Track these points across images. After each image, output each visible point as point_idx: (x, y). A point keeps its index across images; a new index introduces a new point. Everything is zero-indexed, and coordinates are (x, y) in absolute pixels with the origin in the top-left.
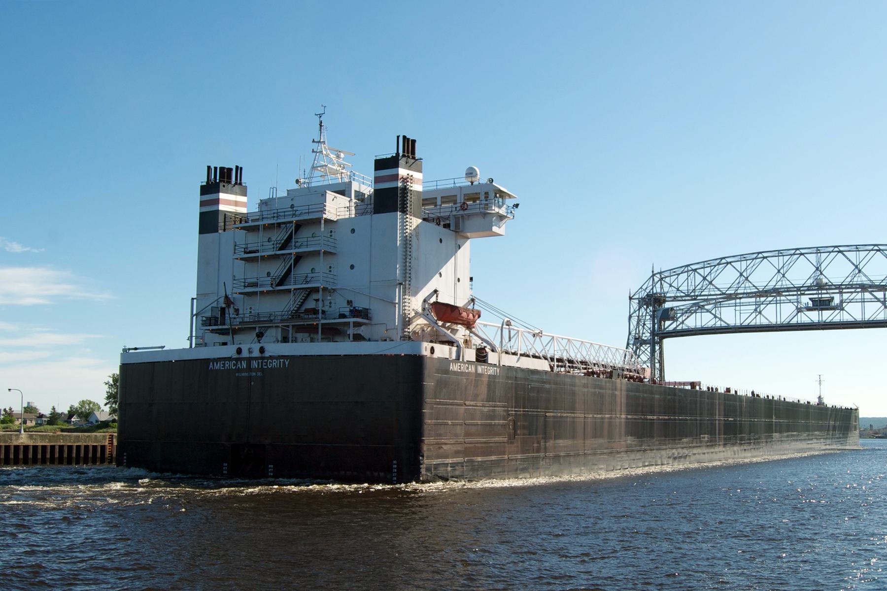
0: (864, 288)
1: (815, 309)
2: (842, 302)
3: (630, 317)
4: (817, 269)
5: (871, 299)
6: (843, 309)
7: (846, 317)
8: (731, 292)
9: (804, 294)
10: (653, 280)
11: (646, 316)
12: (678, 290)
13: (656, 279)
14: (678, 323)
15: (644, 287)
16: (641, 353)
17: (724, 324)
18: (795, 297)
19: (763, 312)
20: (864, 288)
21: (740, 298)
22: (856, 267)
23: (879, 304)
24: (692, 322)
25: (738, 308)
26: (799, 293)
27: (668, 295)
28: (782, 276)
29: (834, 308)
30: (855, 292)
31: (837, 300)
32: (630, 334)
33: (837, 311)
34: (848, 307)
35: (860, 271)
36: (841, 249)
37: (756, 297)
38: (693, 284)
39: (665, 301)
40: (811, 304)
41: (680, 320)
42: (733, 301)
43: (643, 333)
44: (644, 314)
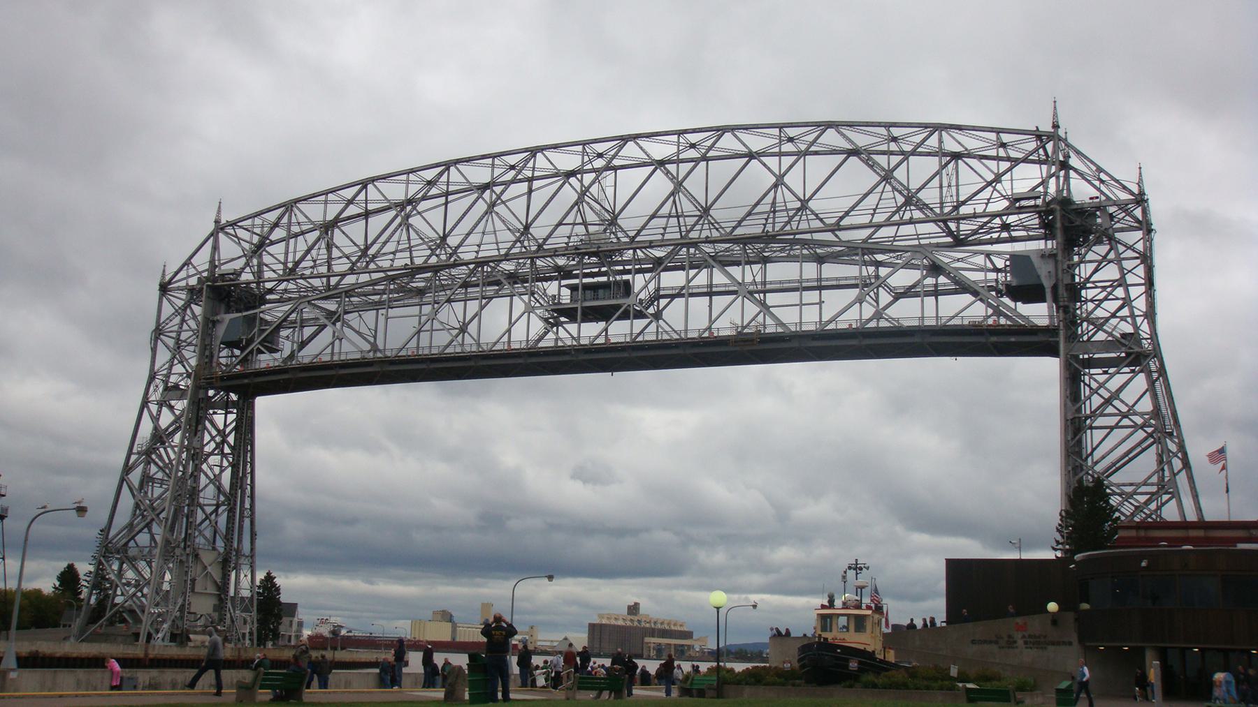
3: (158, 332)
5: (725, 285)
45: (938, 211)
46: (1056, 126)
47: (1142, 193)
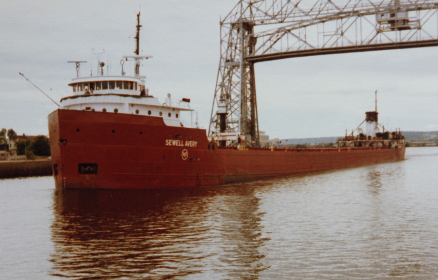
10: (242, 5)
15: (234, 12)
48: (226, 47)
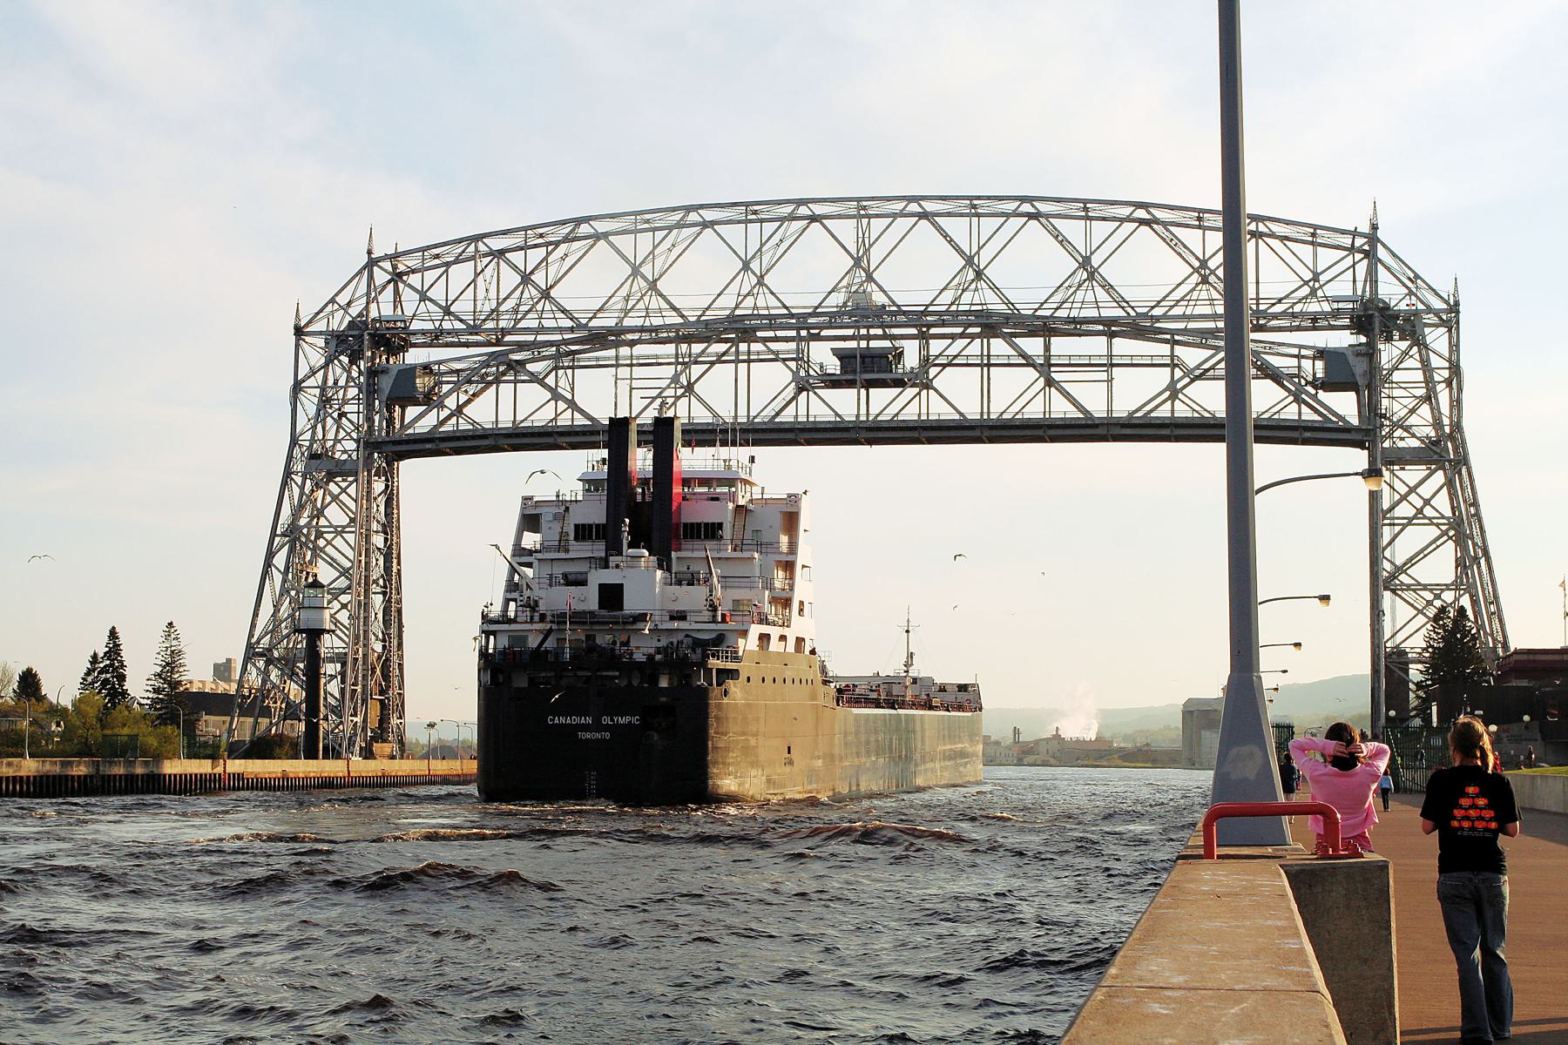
0: (990, 325)
1: (850, 384)
2: (926, 362)
3: (297, 388)
4: (857, 262)
6: (928, 386)
7: (938, 410)
8: (606, 321)
9: (818, 338)
10: (371, 277)
11: (346, 388)
12: (447, 311)
13: (381, 277)
14: (445, 413)
15: (343, 299)
16: (328, 499)
17: (580, 421)
18: (793, 345)
19: (697, 388)
20: (990, 325)
21: (632, 344)
22: (969, 261)
23: (1031, 373)
24: (485, 411)
25: (624, 372)
26: (804, 333)
27: (415, 326)
28: (754, 280)
29: (899, 383)
30: (962, 336)
31: (911, 359)
32: (294, 441)
33: (911, 392)
34: (946, 380)
35: (979, 275)
36: (930, 206)
37: (679, 340)
38: (493, 294)
39: (406, 345)
40: (834, 366)
41: (451, 402)
42: (612, 352)
43: (337, 441)
44: (342, 383)
45: (1254, 307)
46: (1374, 227)
47: (1457, 304)
48: (312, 411)
